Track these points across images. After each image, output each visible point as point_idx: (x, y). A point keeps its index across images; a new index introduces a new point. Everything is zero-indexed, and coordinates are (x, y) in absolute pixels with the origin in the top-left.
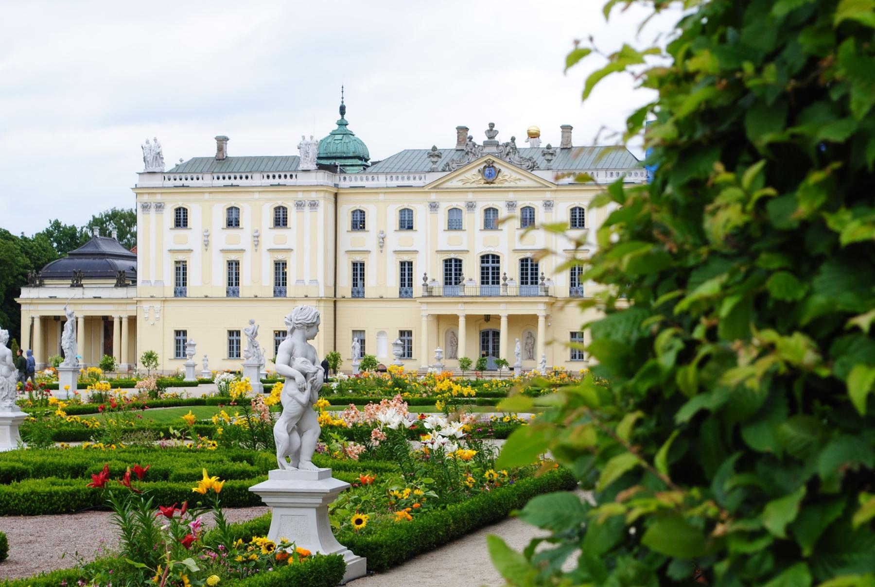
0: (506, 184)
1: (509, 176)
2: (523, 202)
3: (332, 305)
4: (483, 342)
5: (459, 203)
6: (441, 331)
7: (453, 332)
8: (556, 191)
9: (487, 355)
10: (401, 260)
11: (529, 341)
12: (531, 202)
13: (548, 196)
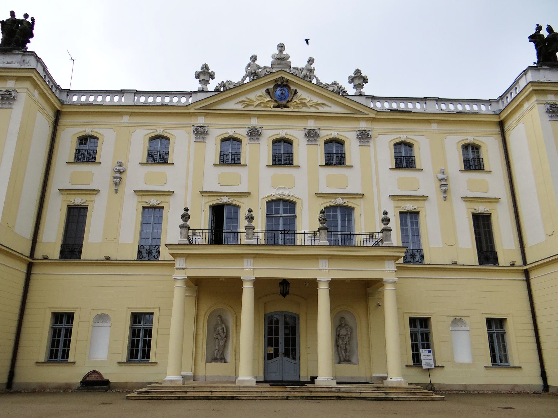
0: (305, 109)
1: (308, 100)
2: (329, 133)
3: (23, 268)
4: (270, 333)
5: (238, 131)
6: (202, 313)
7: (220, 316)
8: (373, 120)
9: (276, 354)
10: (145, 205)
11: (343, 332)
12: (340, 133)
13: (363, 125)
